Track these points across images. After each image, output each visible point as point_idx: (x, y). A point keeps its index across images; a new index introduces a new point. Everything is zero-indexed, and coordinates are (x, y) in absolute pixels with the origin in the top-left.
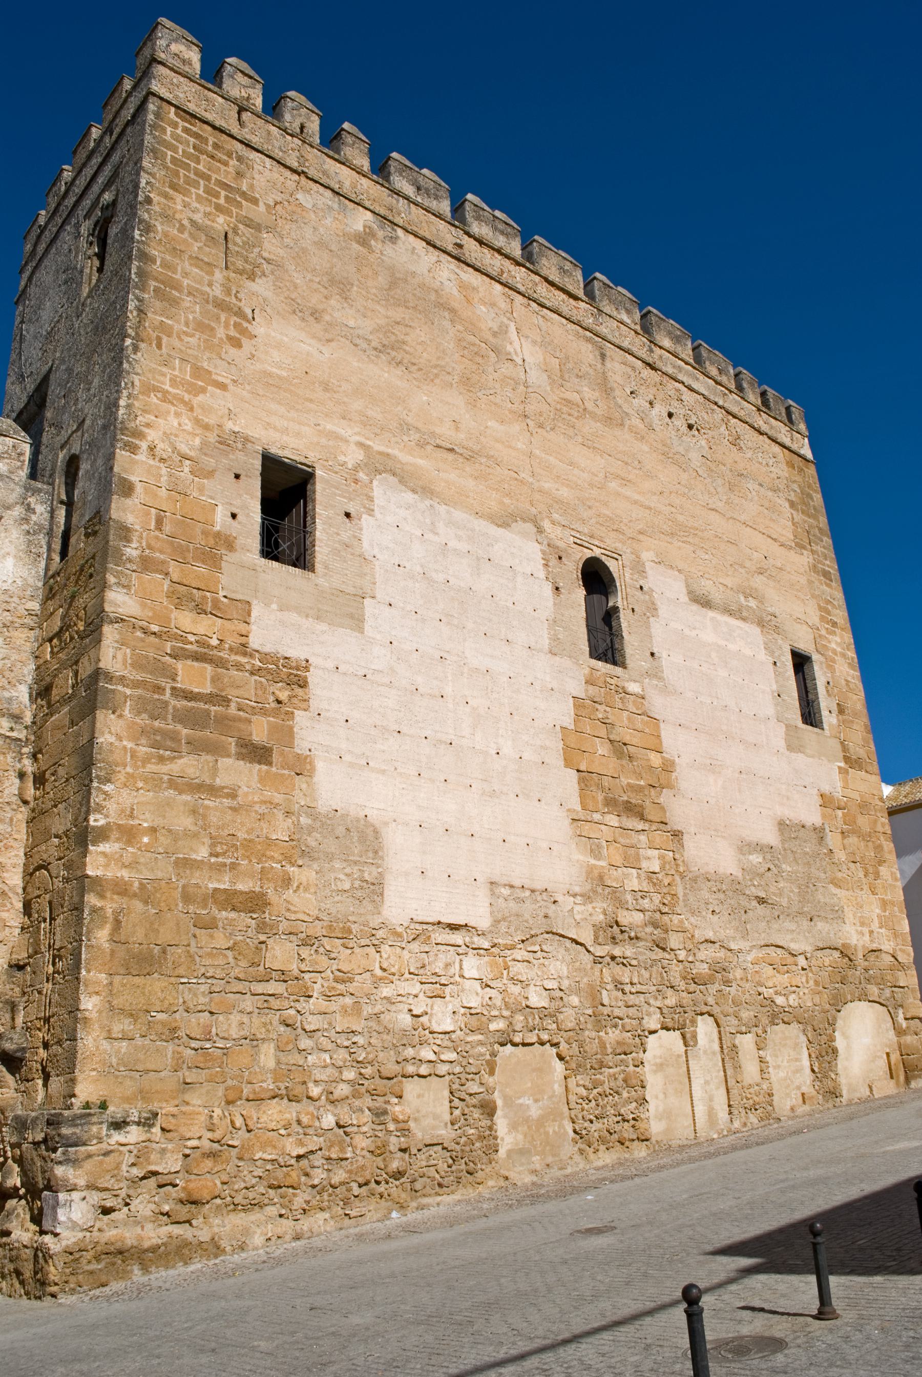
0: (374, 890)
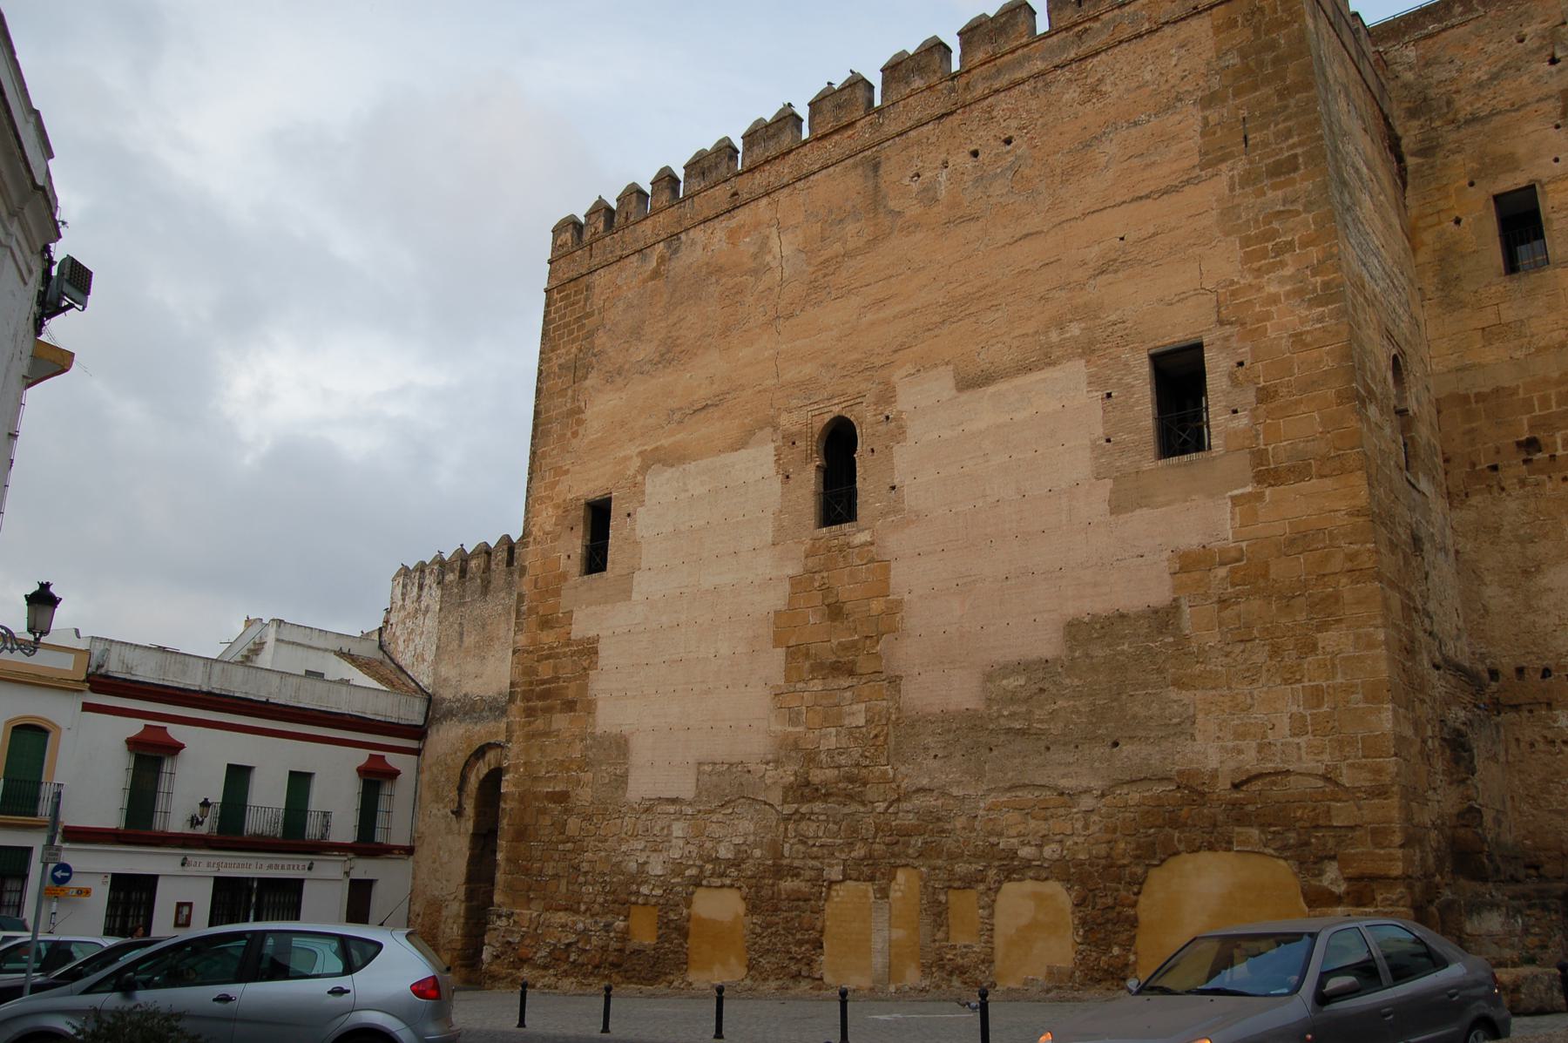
0: (621, 781)
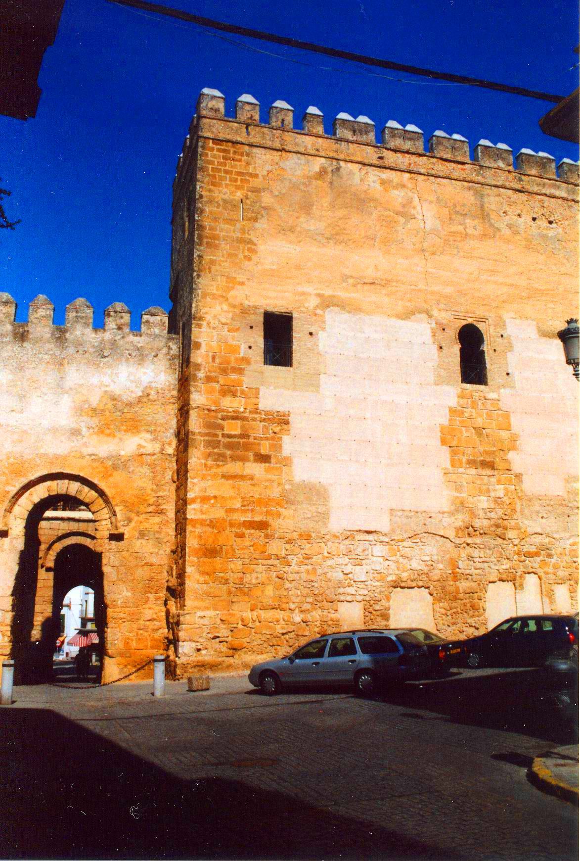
0: (324, 517)
